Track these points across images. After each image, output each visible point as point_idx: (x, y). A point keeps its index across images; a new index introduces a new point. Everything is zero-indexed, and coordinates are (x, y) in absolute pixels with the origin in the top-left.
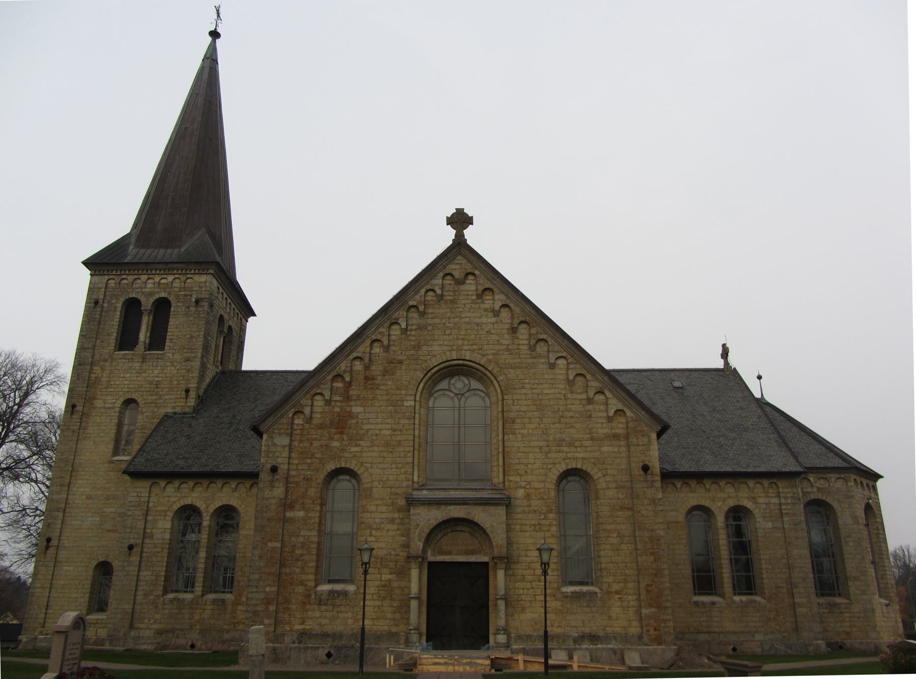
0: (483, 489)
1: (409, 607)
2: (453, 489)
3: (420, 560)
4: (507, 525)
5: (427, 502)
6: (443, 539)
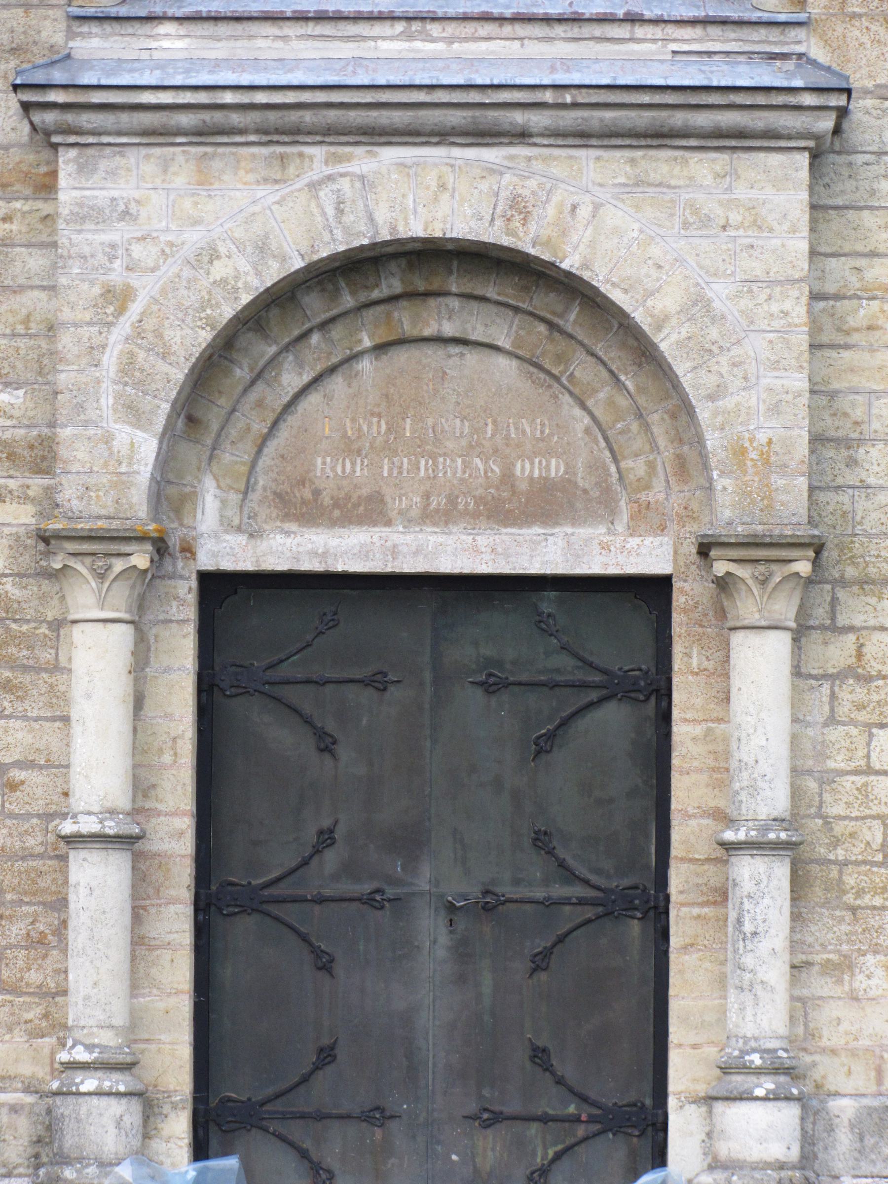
0: (633, 19)
1: (61, 904)
2: (392, 18)
3: (141, 559)
4: (816, 297)
5: (185, 120)
6: (314, 399)
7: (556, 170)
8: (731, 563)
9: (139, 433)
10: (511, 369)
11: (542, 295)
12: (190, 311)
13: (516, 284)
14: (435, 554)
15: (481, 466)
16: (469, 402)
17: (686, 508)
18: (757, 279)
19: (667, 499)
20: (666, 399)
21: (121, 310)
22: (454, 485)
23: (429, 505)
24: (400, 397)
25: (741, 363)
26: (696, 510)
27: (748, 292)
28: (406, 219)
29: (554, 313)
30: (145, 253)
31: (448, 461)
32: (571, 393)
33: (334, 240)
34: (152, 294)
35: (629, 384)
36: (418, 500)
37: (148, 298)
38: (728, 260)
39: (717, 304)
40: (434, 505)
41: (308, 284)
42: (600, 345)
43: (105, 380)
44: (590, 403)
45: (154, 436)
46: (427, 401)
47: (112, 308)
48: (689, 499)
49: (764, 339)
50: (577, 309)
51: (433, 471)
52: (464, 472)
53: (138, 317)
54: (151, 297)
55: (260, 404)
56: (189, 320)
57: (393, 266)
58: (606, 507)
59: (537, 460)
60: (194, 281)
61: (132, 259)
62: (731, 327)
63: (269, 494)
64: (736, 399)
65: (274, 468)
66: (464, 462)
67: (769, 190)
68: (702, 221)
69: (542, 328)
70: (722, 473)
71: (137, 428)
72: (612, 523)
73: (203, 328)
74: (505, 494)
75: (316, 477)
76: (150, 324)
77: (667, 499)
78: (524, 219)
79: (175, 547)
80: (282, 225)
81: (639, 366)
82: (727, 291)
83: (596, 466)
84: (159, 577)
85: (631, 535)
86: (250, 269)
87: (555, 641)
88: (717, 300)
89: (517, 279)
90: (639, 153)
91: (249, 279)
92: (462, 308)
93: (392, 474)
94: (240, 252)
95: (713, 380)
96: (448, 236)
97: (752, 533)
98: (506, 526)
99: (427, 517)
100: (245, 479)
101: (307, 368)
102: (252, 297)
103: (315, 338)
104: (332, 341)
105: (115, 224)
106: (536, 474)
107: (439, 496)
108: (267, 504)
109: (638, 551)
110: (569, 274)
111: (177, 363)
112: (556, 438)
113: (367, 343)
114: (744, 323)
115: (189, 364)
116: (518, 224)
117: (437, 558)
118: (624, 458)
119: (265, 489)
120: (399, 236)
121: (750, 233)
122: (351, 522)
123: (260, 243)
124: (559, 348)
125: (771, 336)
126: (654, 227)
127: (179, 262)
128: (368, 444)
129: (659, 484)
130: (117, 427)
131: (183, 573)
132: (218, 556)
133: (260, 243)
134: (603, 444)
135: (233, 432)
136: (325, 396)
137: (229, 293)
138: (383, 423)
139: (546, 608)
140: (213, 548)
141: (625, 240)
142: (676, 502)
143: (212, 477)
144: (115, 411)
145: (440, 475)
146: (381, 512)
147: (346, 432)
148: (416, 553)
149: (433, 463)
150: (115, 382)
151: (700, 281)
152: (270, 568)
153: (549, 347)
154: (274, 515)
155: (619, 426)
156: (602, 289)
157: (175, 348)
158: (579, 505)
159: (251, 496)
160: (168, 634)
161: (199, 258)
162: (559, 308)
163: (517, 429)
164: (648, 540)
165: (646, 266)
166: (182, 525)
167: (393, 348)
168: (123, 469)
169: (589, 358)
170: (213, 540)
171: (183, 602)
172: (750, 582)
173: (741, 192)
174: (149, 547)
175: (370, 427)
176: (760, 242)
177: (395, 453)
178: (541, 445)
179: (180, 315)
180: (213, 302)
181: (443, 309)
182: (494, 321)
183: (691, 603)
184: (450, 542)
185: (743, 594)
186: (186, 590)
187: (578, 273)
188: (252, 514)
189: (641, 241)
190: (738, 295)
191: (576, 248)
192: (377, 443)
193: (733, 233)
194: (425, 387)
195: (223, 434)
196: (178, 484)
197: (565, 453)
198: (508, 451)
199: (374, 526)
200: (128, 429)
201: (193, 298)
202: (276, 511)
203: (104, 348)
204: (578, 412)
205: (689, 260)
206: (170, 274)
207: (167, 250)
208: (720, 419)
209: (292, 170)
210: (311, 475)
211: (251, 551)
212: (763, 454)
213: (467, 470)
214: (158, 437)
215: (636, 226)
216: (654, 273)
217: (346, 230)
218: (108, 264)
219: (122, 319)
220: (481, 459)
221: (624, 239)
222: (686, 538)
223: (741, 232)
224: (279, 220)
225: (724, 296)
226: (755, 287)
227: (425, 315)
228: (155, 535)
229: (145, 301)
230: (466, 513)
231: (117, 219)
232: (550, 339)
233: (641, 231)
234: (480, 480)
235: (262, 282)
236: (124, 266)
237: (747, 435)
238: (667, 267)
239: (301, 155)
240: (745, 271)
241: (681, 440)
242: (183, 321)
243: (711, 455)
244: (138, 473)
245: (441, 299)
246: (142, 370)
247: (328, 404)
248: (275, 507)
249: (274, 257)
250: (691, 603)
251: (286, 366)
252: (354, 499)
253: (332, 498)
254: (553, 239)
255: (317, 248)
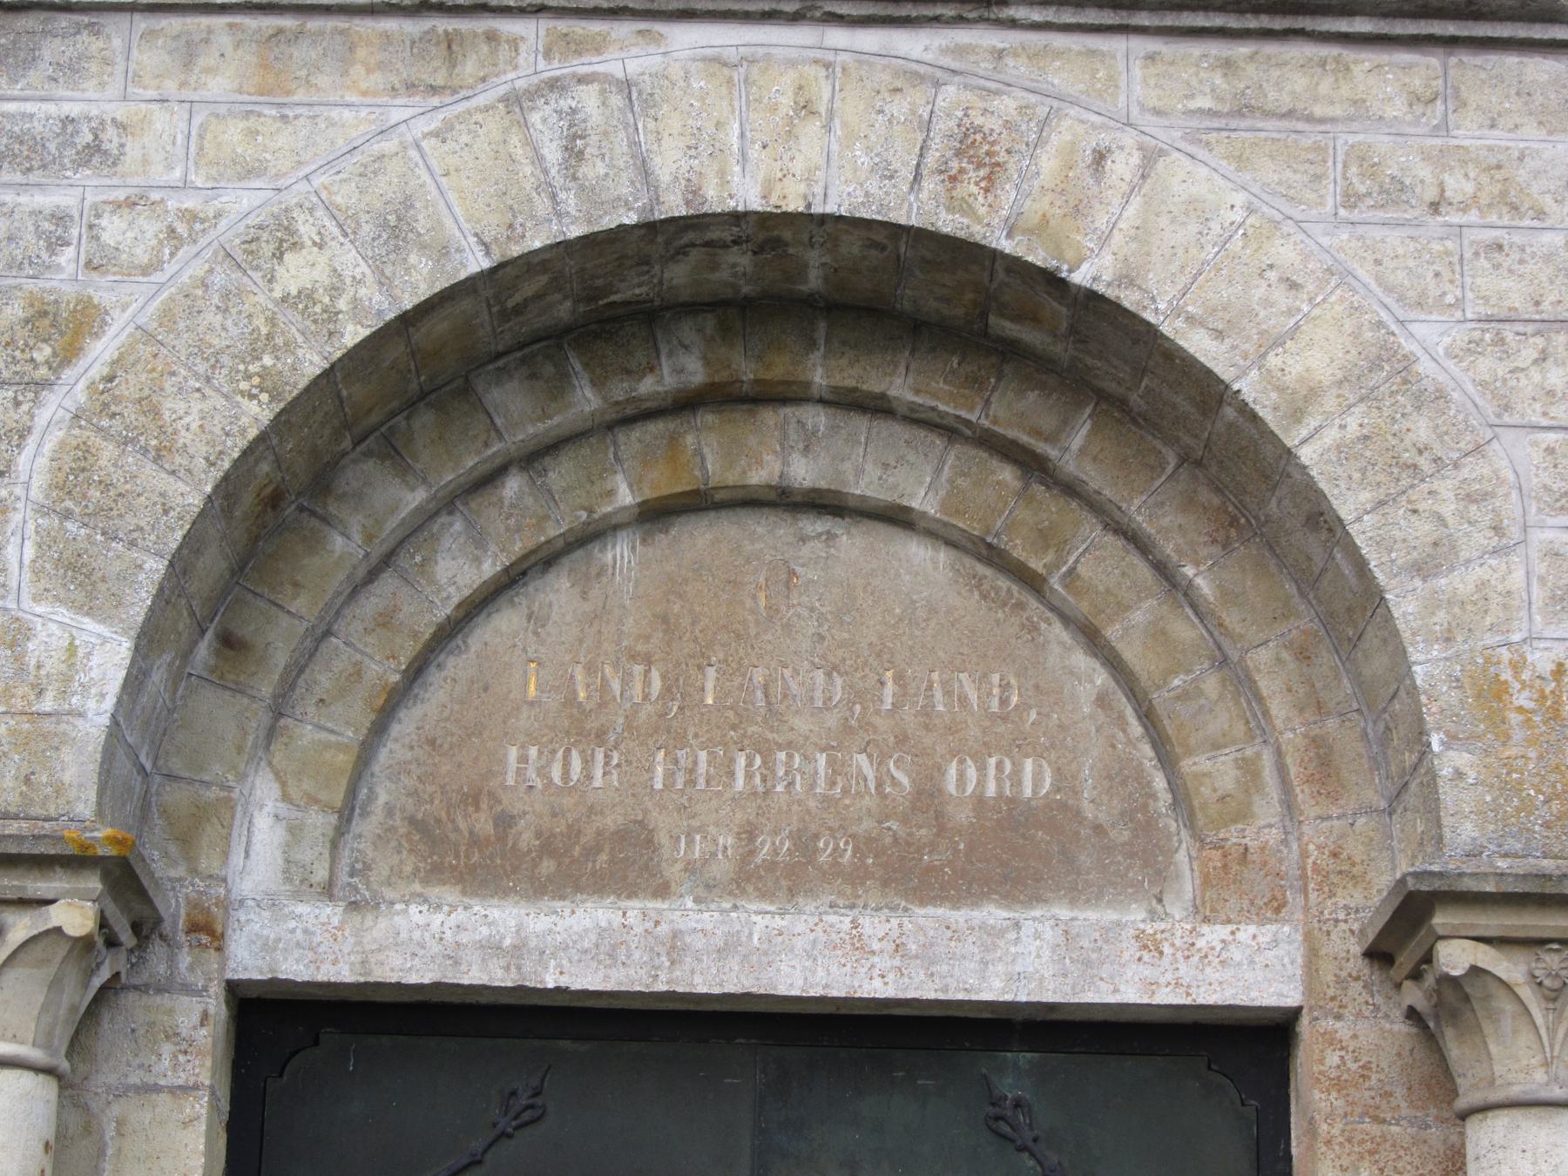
6: (505, 622)
7: (1060, 78)
8: (1483, 947)
9: (89, 624)
10: (936, 568)
11: (1010, 395)
12: (225, 359)
13: (953, 372)
14: (766, 953)
15: (869, 772)
16: (846, 635)
17: (1335, 855)
18: (1513, 315)
19: (1285, 842)
20: (1286, 617)
21: (68, 354)
22: (809, 812)
23: (752, 853)
24: (693, 623)
25: (1486, 496)
26: (1357, 859)
27: (1494, 343)
28: (722, 174)
29: (1036, 433)
30: (130, 234)
31: (797, 759)
32: (1066, 619)
33: (559, 215)
34: (141, 321)
35: (1204, 586)
36: (730, 841)
37: (130, 329)
38: (1446, 275)
39: (1425, 366)
40: (764, 853)
41: (500, 363)
42: (1137, 502)
43: (20, 505)
44: (1112, 633)
45: (124, 632)
46: (753, 632)
47: (47, 351)
48: (1343, 836)
49: (1535, 444)
50: (1088, 426)
51: (764, 780)
52: (833, 784)
53: (106, 371)
54: (138, 327)
55: (385, 620)
56: (220, 378)
57: (687, 330)
58: (1146, 864)
59: (993, 761)
60: (238, 295)
61: (102, 247)
62: (1460, 417)
63: (398, 823)
64: (1478, 573)
65: (413, 767)
66: (831, 762)
67: (1531, 131)
68: (1387, 192)
69: (1007, 474)
70: (1452, 740)
71: (87, 614)
72: (1160, 901)
73: (252, 397)
74: (923, 832)
75: (505, 788)
76: (129, 385)
77: (1285, 842)
78: (989, 178)
79: (175, 923)
80: (443, 180)
81: (1224, 547)
82: (1447, 340)
83: (1121, 776)
84: (136, 988)
85: (1206, 920)
86: (368, 271)
87: (1032, 1163)
88: (1424, 358)
89: (955, 361)
90: (1242, 50)
91: (363, 292)
92: (834, 429)
93: (674, 784)
94: (346, 235)
95: (1423, 530)
96: (817, 209)
97: (1535, 872)
98: (923, 903)
99: (748, 880)
100: (344, 782)
101: (493, 548)
102: (367, 332)
103: (513, 485)
104: (549, 491)
105: (68, 173)
106: (991, 790)
107: (776, 832)
108: (393, 844)
109: (1224, 955)
110: (1092, 301)
111: (189, 471)
112: (1033, 716)
113: (626, 497)
114: (1490, 410)
115: (216, 474)
116: (974, 189)
117: (769, 964)
118: (1190, 752)
119: (390, 811)
120: (705, 209)
121: (1493, 218)
122: (578, 889)
123: (392, 219)
124: (1045, 516)
125: (1551, 437)
126: (1280, 203)
127: (208, 254)
128: (621, 720)
129: (1267, 809)
130: (39, 610)
131: (191, 979)
132: (275, 949)
133: (392, 219)
134: (1136, 729)
135: (323, 678)
136: (529, 618)
137: (315, 322)
138: (655, 675)
139: (1009, 1087)
140: (265, 932)
141: (1216, 227)
142: (1315, 835)
143: (271, 776)
144: (37, 573)
145: (779, 788)
146: (646, 867)
147: (575, 693)
148: (722, 952)
149: (764, 763)
150: (42, 510)
151: (1384, 315)
152: (393, 978)
153: (1024, 514)
154: (408, 869)
155: (1176, 682)
156: (1166, 329)
157: (184, 438)
158: (1085, 860)
159: (358, 826)
160: (147, 1117)
161: (254, 246)
162: (1048, 422)
163: (948, 693)
164: (1246, 932)
165: (1264, 284)
166: (194, 871)
167: (683, 519)
168: (47, 704)
169: (1109, 538)
170: (266, 914)
171: (186, 1047)
172: (1526, 993)
173: (1469, 133)
174: (94, 883)
175: (626, 682)
176: (1517, 238)
177: (681, 740)
178: (1001, 729)
179: (202, 368)
180: (279, 341)
181: (792, 429)
182: (902, 457)
183: (1354, 1067)
184: (800, 927)
185: (1507, 1024)
186: (196, 1018)
187: (1111, 293)
188: (359, 866)
189: (1250, 231)
190: (1473, 348)
191: (1105, 240)
192: (643, 715)
193: (1455, 218)
194: (749, 603)
195: (301, 682)
196: (191, 781)
197: (1053, 746)
198: (928, 741)
199: (629, 897)
200: (64, 614)
201: (234, 331)
202: (413, 858)
203: (22, 437)
204: (1081, 660)
205: (1360, 273)
206: (185, 278)
207: (182, 229)
208: (1441, 616)
209: (469, 68)
210: (493, 783)
211: (352, 940)
212: (1543, 697)
213: (839, 779)
214: (133, 633)
215: (1239, 198)
216: (1281, 297)
217: (586, 192)
218: (45, 255)
219: (68, 374)
220: (870, 756)
221: (1212, 224)
222: (1337, 921)
223: (1473, 216)
224: (438, 171)
225: (1441, 350)
226: (1508, 332)
227: (753, 441)
228: (110, 851)
229: (123, 336)
230: (834, 872)
231: (73, 161)
232: (1023, 494)
233: (1251, 210)
234: (867, 801)
235: (394, 299)
236: (82, 262)
237: (1505, 654)
238: (1310, 287)
239: (491, 37)
240: (1486, 299)
241: (1319, 706)
242: (208, 380)
243: (1423, 699)
244: (81, 715)
245: (787, 411)
246: (106, 486)
247: (536, 633)
248: (411, 851)
249: (423, 247)
250: (1354, 1067)
251: (446, 542)
252: (587, 838)
253: (538, 835)
254: (1052, 222)
255: (519, 230)
